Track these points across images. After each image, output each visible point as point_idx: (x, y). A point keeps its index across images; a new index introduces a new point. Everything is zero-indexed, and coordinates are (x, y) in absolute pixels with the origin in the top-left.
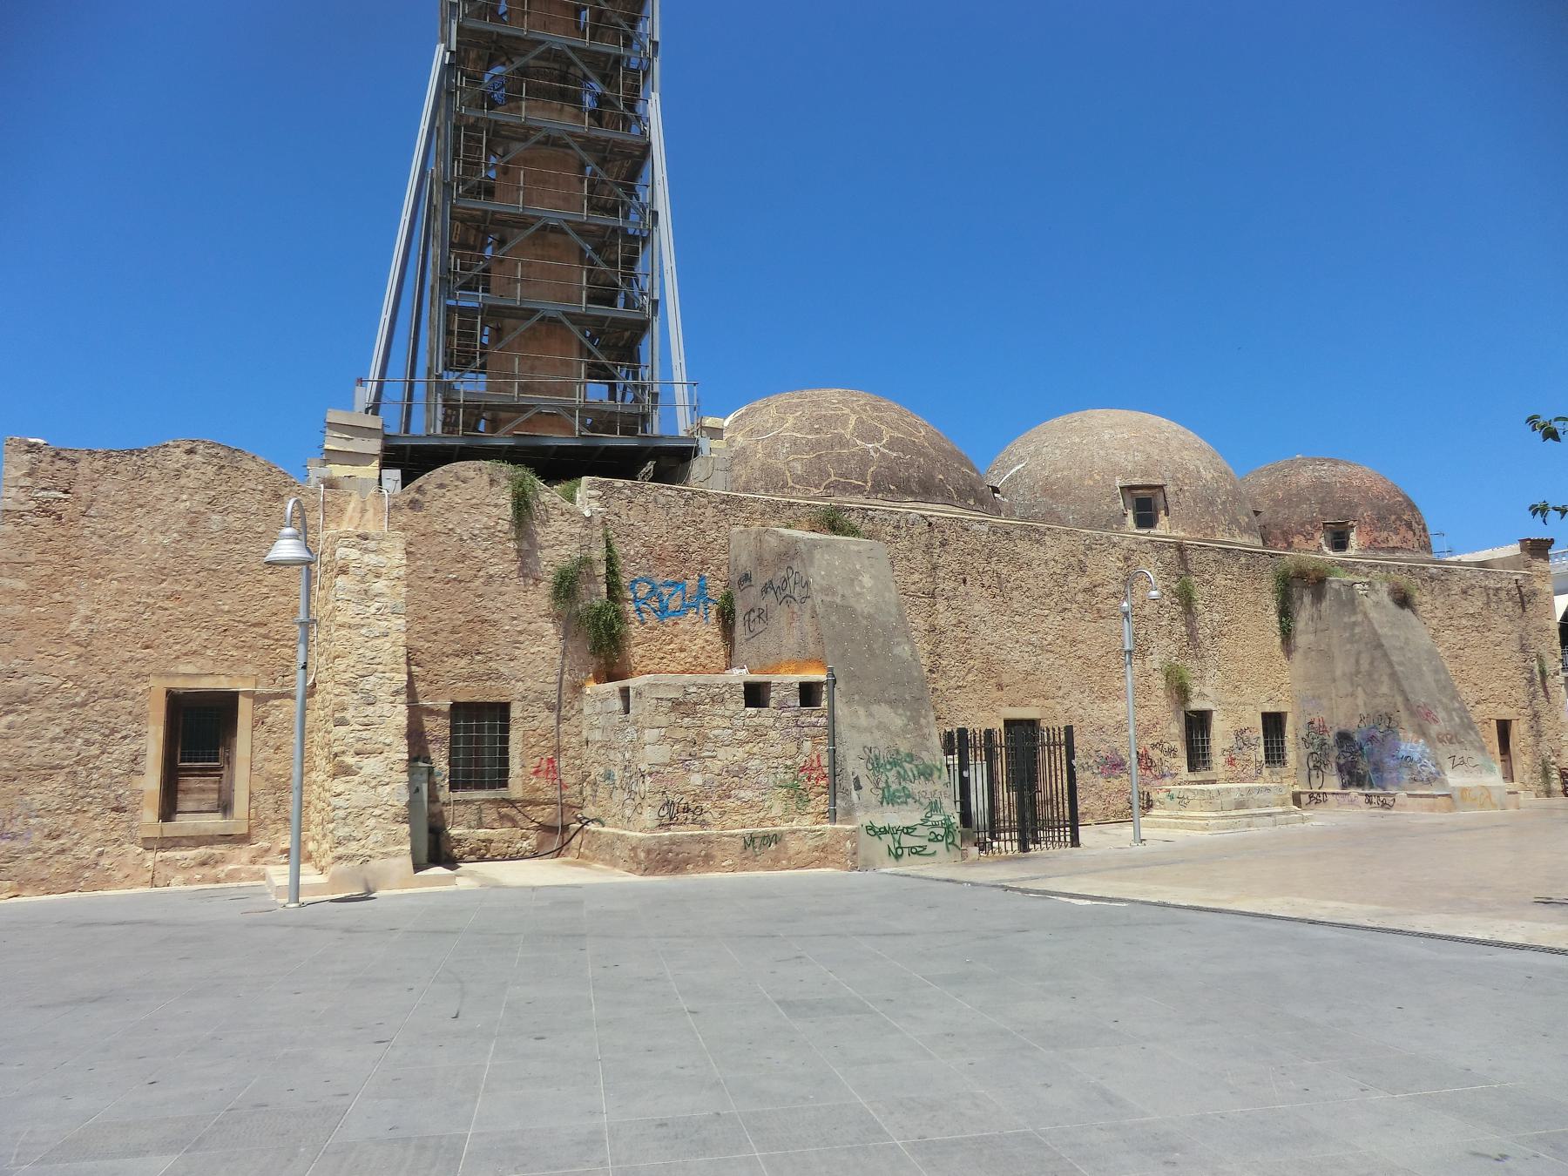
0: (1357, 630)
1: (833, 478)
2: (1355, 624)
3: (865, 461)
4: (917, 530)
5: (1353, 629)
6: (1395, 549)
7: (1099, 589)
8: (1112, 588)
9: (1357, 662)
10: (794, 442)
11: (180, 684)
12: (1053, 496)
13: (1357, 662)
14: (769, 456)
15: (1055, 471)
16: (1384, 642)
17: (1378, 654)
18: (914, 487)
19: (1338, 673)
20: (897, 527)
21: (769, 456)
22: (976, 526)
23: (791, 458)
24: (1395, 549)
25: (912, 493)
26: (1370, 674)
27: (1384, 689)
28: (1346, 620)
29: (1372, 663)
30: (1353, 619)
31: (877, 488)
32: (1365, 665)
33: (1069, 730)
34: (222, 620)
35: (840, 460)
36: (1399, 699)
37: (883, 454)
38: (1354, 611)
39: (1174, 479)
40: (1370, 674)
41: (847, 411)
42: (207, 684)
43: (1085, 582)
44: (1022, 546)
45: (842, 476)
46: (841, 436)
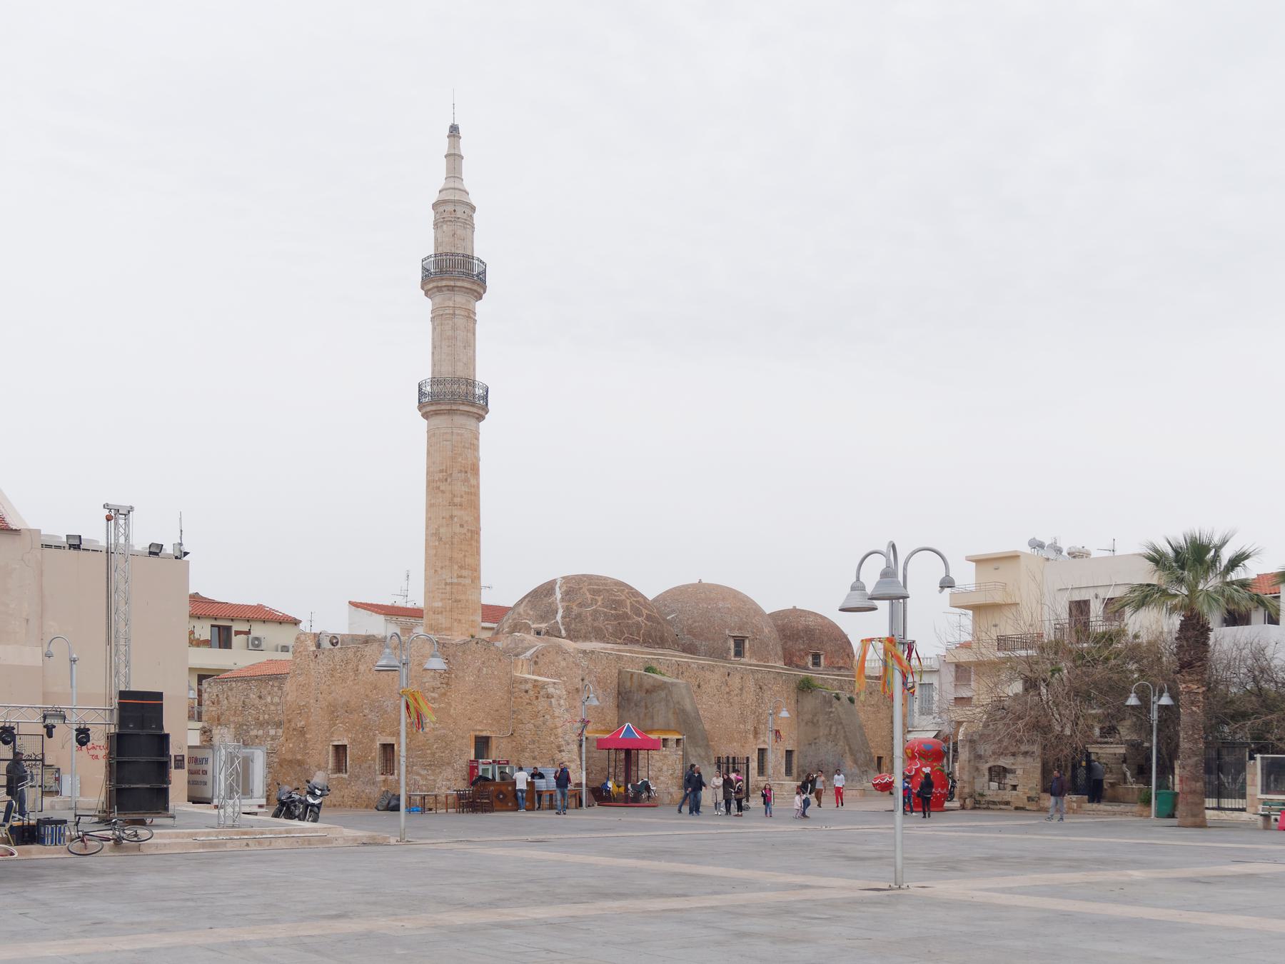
0: (832, 715)
1: (626, 635)
2: (831, 712)
3: (638, 626)
4: (674, 668)
5: (829, 714)
6: (840, 668)
7: (732, 693)
8: (736, 692)
9: (830, 729)
10: (605, 614)
11: (477, 733)
12: (694, 636)
13: (830, 729)
14: (594, 620)
15: (695, 622)
16: (843, 721)
17: (840, 727)
18: (658, 640)
19: (821, 734)
20: (668, 667)
21: (594, 620)
22: (693, 665)
23: (606, 622)
24: (840, 668)
25: (658, 644)
26: (835, 735)
27: (841, 743)
28: (827, 710)
29: (836, 731)
30: (830, 710)
31: (644, 642)
32: (833, 731)
33: (748, 759)
34: (487, 709)
35: (628, 626)
36: (847, 748)
37: (646, 624)
38: (831, 707)
39: (753, 632)
40: (835, 735)
41: (623, 597)
42: (484, 734)
43: (727, 690)
44: (708, 673)
45: (631, 634)
46: (627, 613)
